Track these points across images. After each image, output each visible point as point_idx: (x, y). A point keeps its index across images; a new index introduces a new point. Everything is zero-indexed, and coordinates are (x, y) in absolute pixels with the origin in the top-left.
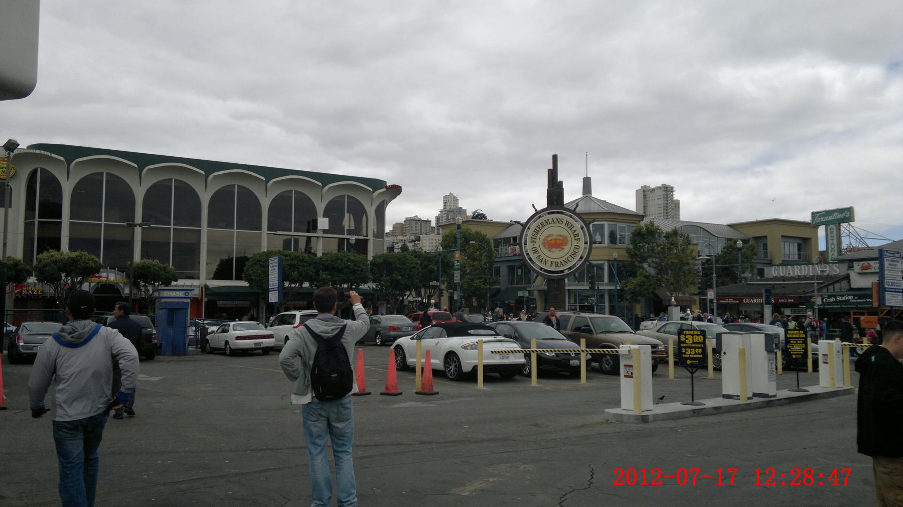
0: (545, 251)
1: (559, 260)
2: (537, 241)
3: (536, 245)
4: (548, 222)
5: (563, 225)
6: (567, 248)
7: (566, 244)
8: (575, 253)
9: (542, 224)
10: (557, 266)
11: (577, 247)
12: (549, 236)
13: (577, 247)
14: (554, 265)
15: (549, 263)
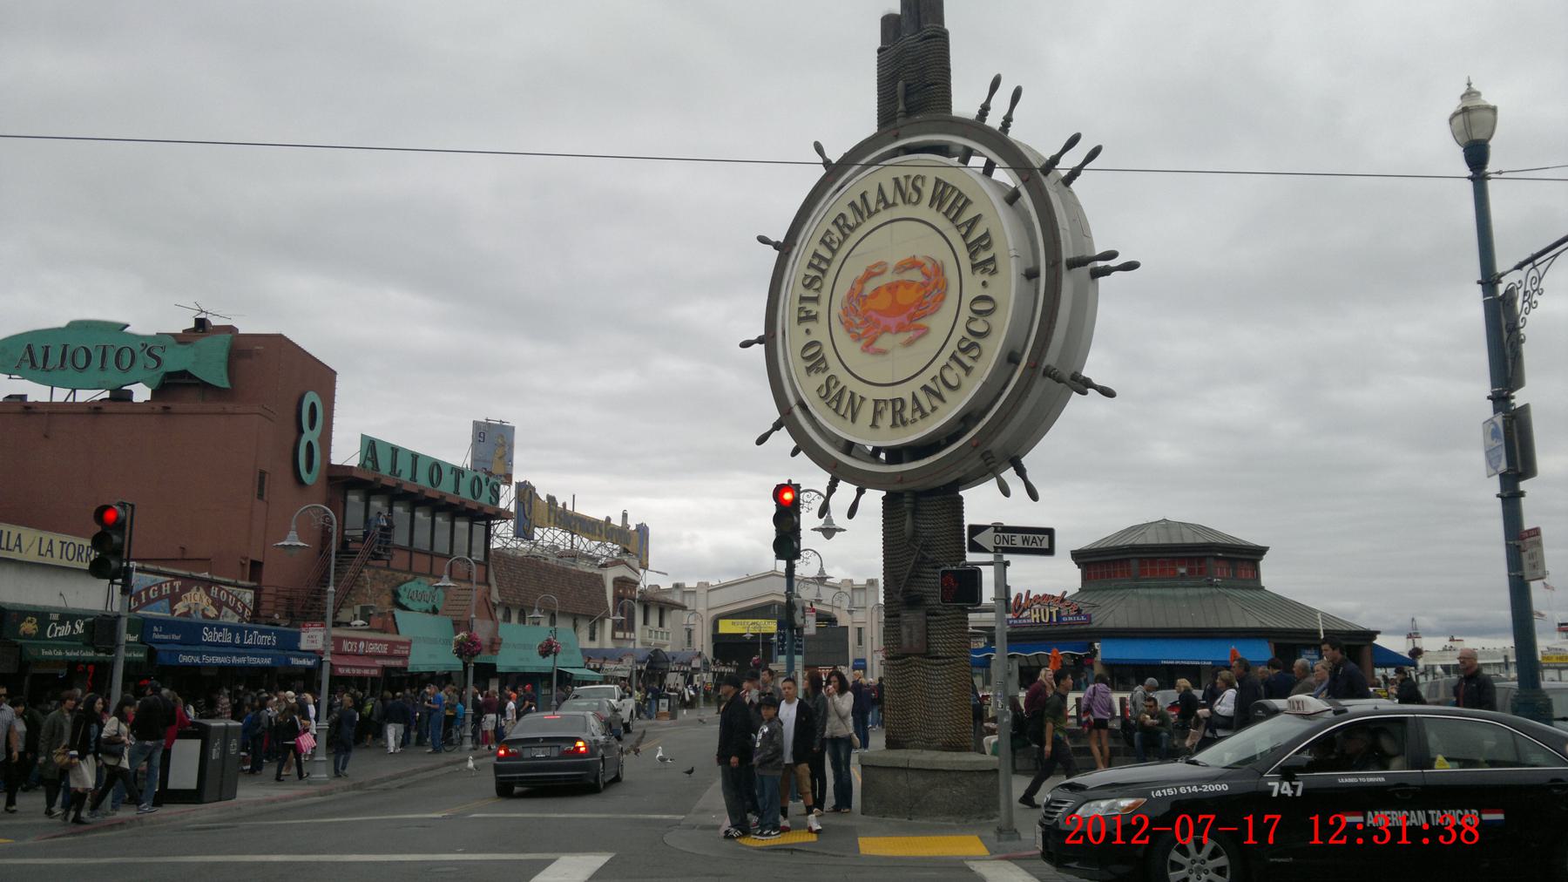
0: (851, 350)
1: (904, 392)
2: (820, 309)
3: (819, 332)
4: (862, 209)
5: (924, 211)
6: (939, 324)
7: (936, 309)
8: (972, 345)
9: (840, 221)
10: (899, 421)
11: (984, 306)
12: (870, 274)
13: (984, 306)
14: (888, 415)
15: (866, 413)
